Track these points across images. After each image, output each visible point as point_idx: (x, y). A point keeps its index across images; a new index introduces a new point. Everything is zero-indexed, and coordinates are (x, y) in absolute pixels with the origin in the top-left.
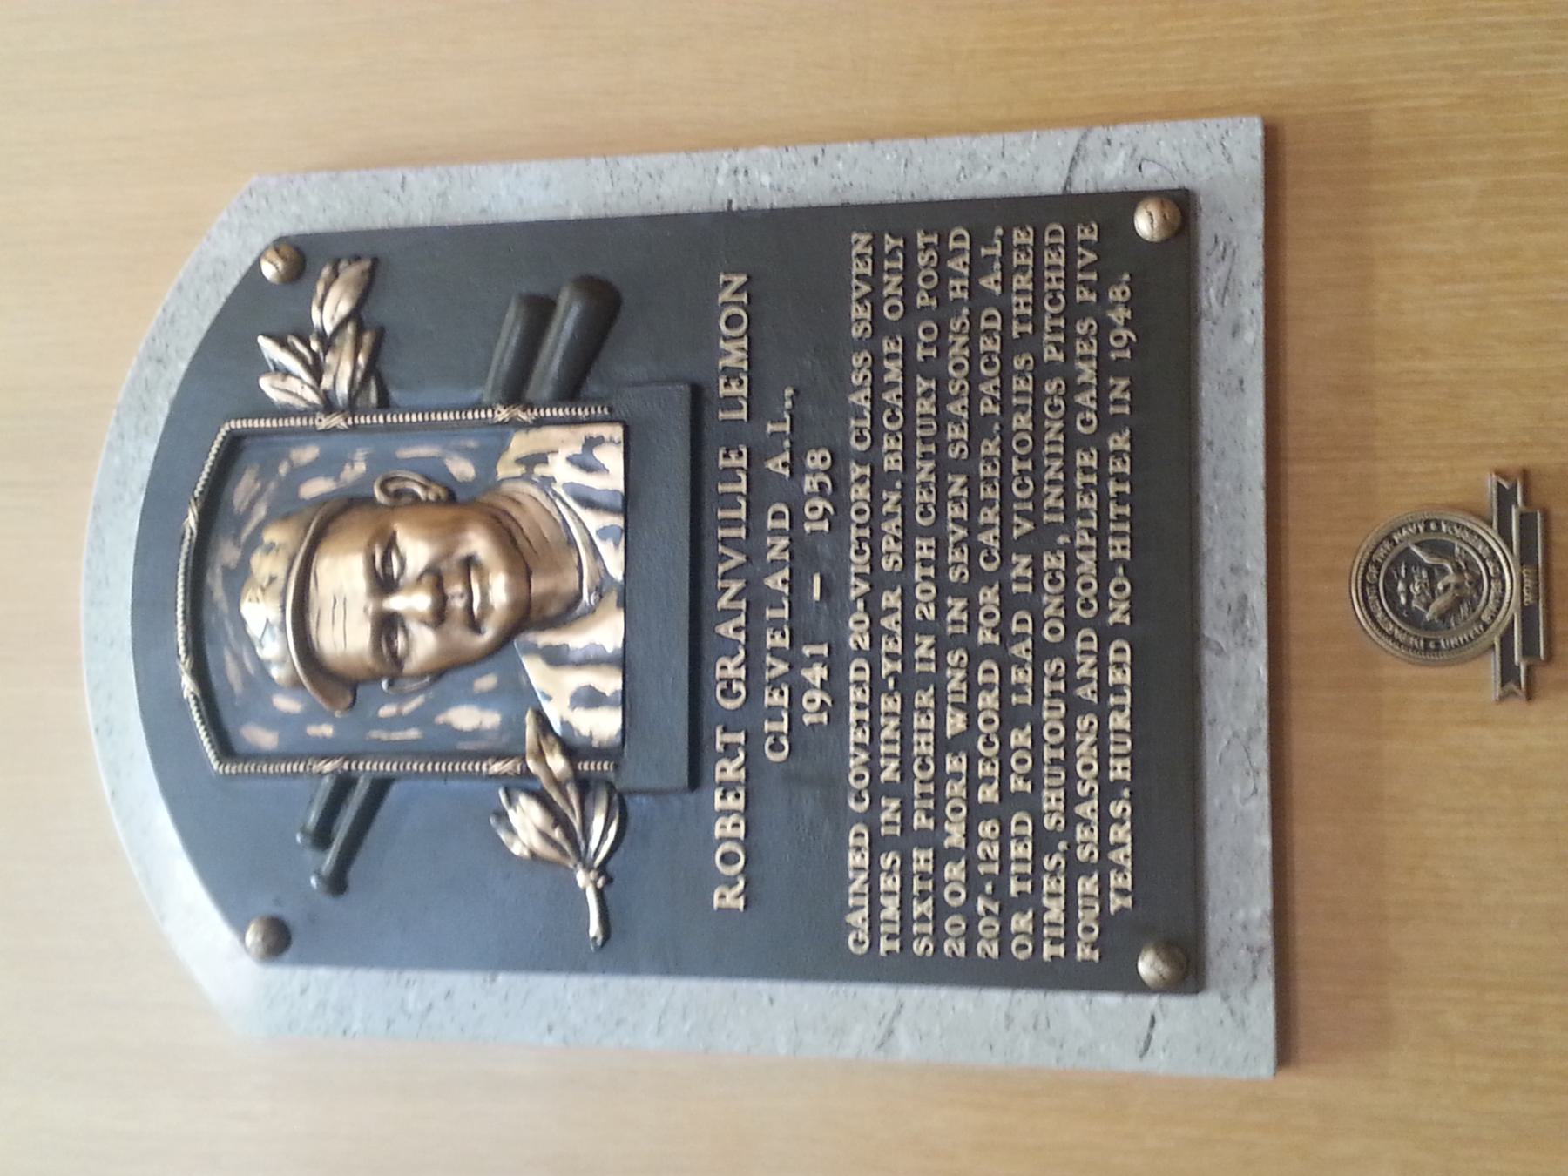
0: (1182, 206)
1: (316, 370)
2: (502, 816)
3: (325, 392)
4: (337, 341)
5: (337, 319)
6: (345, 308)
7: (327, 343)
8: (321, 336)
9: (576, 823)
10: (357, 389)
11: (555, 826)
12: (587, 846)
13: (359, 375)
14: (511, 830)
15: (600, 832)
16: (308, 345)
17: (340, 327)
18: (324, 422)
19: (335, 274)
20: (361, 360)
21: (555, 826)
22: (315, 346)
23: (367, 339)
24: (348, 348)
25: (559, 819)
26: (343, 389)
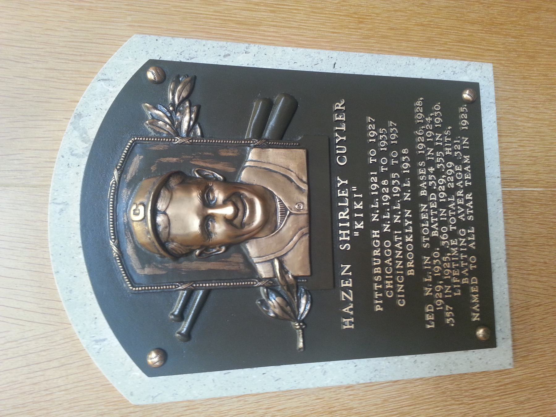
0: (474, 87)
1: (171, 118)
2: (264, 303)
6: (184, 94)
7: (176, 109)
8: (173, 104)
10: (190, 129)
11: (287, 306)
12: (298, 314)
13: (192, 123)
17: (182, 102)
20: (193, 116)
22: (171, 108)
23: (194, 109)
24: (188, 111)
25: (289, 304)
26: (185, 126)
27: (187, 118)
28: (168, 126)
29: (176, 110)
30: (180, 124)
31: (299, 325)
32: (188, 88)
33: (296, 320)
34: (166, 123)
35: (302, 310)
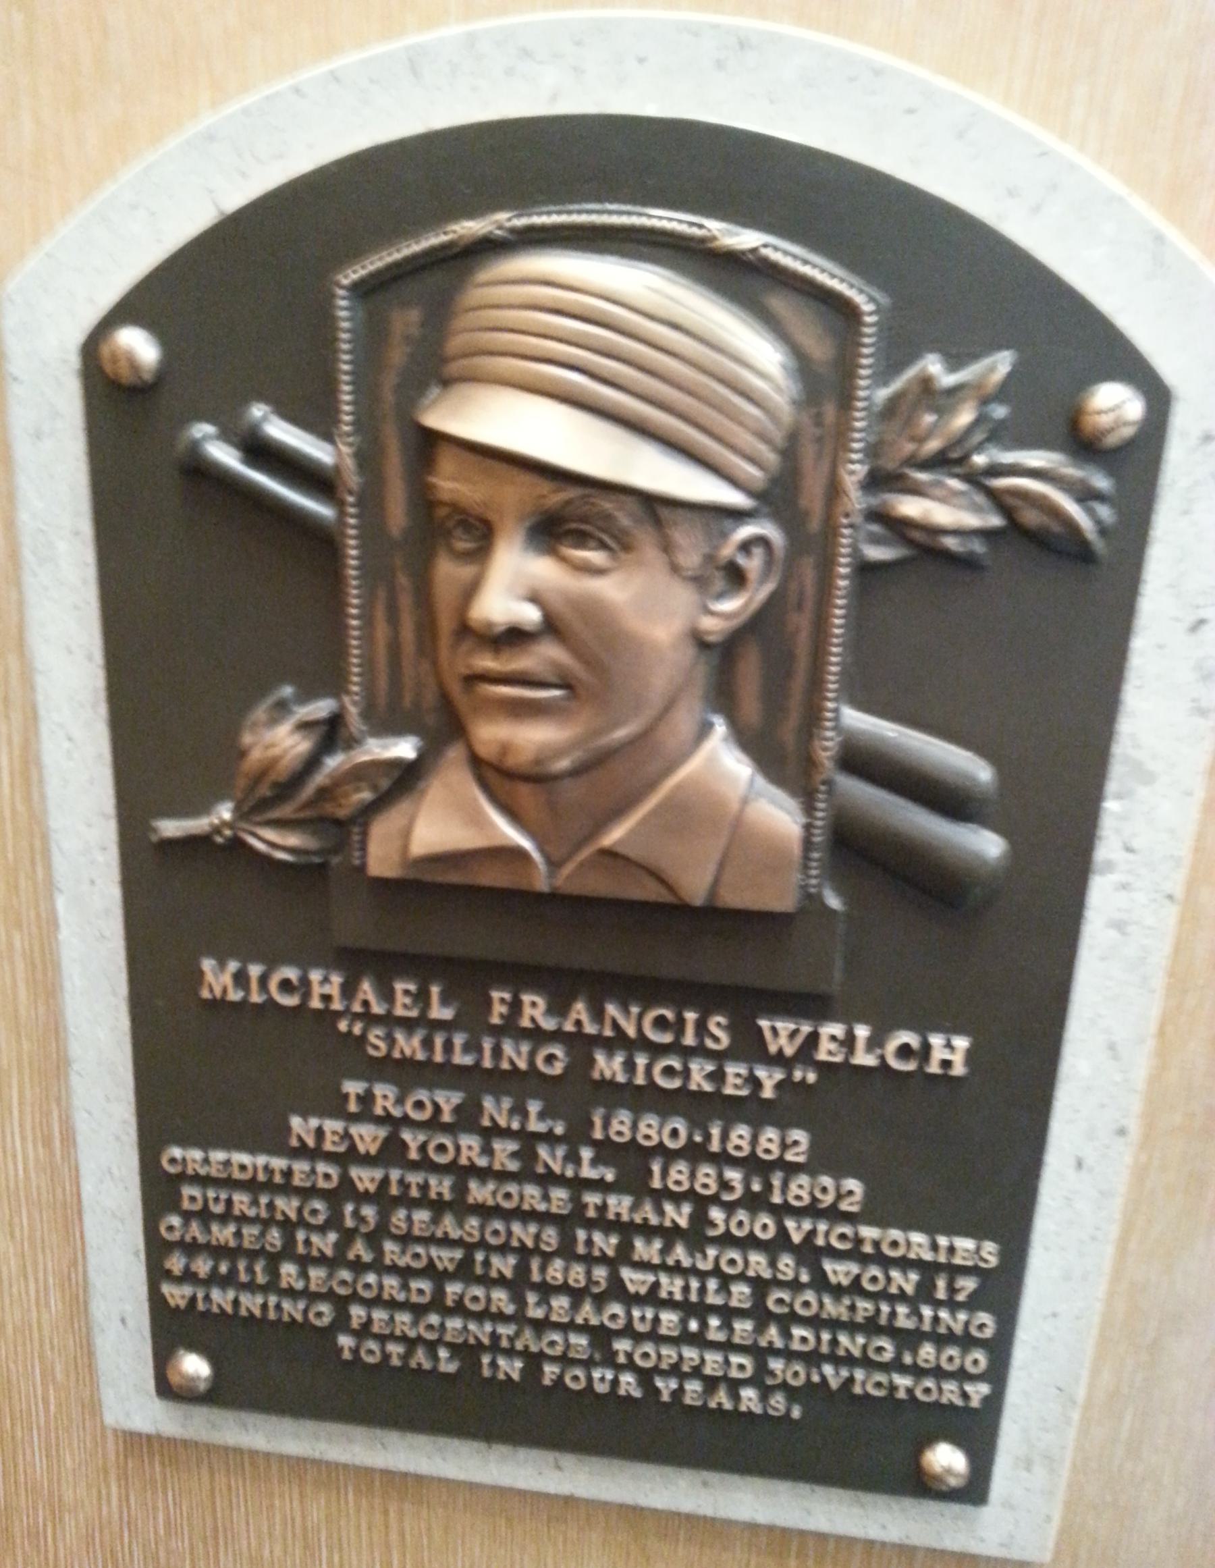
1: (941, 461)
3: (900, 477)
4: (980, 499)
5: (1011, 501)
6: (1031, 517)
9: (286, 811)
10: (898, 528)
12: (259, 824)
13: (917, 535)
14: (273, 721)
15: (276, 841)
16: (979, 448)
18: (855, 471)
19: (1085, 495)
21: (276, 785)
22: (980, 460)
27: (940, 514)
28: (909, 447)
29: (975, 479)
30: (916, 491)
31: (225, 824)
32: (1056, 528)
33: (242, 813)
34: (921, 440)
35: (270, 834)
